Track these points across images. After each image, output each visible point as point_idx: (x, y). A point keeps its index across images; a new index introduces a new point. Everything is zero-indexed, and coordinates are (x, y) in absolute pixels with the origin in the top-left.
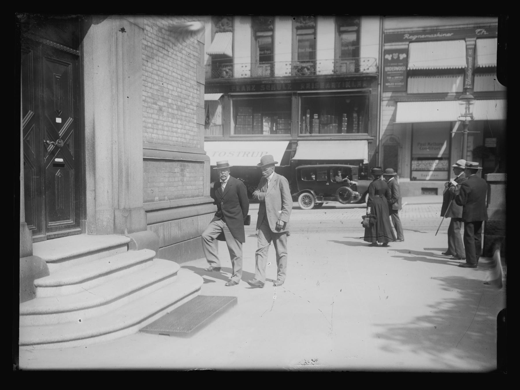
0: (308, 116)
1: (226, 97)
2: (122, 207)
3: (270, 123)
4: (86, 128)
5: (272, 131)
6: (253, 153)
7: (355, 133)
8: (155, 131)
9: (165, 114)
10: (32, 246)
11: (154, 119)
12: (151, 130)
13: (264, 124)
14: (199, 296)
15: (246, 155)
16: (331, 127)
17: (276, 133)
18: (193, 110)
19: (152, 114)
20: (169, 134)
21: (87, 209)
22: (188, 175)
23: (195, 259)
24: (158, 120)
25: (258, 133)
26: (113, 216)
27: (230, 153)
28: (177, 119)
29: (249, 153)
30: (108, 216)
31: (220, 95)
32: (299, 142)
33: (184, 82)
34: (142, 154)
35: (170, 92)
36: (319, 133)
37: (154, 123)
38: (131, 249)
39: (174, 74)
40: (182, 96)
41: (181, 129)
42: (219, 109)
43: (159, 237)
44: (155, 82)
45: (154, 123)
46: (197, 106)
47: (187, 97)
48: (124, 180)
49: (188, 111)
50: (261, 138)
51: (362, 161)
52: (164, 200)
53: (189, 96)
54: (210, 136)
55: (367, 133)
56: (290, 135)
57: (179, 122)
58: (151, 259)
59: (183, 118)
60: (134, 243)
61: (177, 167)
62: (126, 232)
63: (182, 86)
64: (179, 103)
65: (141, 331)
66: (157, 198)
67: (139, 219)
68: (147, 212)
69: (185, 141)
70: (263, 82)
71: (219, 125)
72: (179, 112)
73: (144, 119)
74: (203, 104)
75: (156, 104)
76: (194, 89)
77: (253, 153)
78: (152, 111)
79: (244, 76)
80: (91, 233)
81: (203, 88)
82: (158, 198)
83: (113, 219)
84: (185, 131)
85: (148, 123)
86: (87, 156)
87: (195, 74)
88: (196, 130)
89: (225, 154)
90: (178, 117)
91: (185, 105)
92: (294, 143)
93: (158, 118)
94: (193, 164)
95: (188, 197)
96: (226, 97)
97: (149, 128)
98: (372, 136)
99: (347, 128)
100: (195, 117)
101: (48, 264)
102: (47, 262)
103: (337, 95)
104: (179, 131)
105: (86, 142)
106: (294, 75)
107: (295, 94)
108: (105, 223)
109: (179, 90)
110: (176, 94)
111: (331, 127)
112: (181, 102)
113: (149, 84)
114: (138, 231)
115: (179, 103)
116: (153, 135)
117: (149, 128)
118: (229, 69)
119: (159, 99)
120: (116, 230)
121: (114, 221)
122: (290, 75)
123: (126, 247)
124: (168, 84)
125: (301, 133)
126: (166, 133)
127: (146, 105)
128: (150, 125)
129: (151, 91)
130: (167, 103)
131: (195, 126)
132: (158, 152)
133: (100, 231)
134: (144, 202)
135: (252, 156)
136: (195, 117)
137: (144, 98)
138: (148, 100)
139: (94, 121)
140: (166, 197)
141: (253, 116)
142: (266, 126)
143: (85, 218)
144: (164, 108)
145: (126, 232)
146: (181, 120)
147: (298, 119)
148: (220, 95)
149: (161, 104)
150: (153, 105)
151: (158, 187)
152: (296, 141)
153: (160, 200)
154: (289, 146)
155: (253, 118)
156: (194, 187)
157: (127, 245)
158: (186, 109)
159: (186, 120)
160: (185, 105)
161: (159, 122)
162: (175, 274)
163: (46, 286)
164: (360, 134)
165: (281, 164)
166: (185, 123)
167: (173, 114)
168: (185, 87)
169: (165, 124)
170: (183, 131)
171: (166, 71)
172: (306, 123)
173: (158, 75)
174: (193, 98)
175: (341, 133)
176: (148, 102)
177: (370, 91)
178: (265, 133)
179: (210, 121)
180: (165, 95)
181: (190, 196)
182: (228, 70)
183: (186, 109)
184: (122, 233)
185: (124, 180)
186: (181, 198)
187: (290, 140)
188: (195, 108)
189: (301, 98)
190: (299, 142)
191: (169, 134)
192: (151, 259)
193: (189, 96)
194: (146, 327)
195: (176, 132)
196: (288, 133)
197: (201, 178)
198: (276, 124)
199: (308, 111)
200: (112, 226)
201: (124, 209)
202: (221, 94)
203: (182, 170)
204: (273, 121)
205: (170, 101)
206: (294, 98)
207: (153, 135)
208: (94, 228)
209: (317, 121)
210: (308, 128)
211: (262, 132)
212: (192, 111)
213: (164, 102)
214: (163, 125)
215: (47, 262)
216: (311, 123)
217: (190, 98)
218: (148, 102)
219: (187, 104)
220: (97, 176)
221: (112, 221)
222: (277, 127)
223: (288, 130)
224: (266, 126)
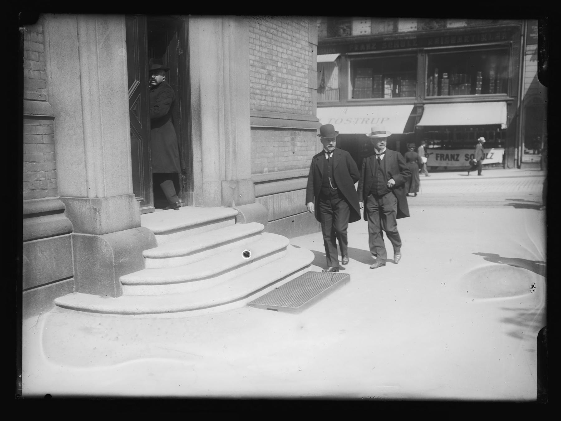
0: (436, 75)
1: (343, 58)
2: (229, 179)
3: (392, 86)
4: (192, 96)
5: (394, 94)
6: (373, 119)
7: (491, 93)
8: (264, 98)
9: (274, 79)
10: (140, 217)
11: (262, 84)
12: (260, 97)
13: (386, 86)
14: (309, 272)
15: (364, 122)
16: (463, 88)
17: (399, 96)
18: (304, 73)
19: (260, 79)
20: (279, 100)
21: (195, 180)
22: (299, 144)
23: (307, 234)
25: (379, 97)
26: (221, 188)
27: (347, 120)
29: (369, 119)
30: (216, 188)
31: (337, 55)
32: (426, 106)
33: (294, 44)
34: (249, 122)
35: (280, 55)
36: (449, 94)
37: (263, 89)
38: (239, 222)
39: (284, 35)
40: (292, 58)
41: (292, 94)
42: (336, 71)
43: (268, 209)
44: (263, 44)
46: (308, 69)
47: (298, 60)
48: (231, 150)
49: (299, 74)
50: (382, 103)
51: (499, 126)
52: (274, 171)
53: (300, 58)
54: (325, 101)
55: (506, 92)
56: (414, 98)
57: (289, 87)
58: (259, 233)
59: (294, 82)
60: (242, 216)
61: (287, 136)
62: (234, 205)
63: (293, 48)
64: (289, 67)
65: (249, 305)
66: (266, 169)
67: (247, 190)
68: (256, 183)
70: (385, 39)
71: (336, 89)
72: (290, 76)
73: (251, 85)
74: (315, 67)
75: (264, 68)
76: (305, 50)
77: (373, 119)
78: (260, 76)
79: (363, 33)
80: (199, 205)
81: (315, 49)
83: (220, 190)
84: (296, 97)
85: (256, 89)
86: (193, 126)
87: (307, 34)
88: (308, 95)
89: (342, 120)
90: (289, 81)
91: (296, 69)
92: (420, 107)
93: (266, 83)
94: (305, 132)
95: (299, 168)
96: (343, 58)
97: (257, 94)
98: (512, 97)
99: (482, 88)
100: (307, 81)
101: (157, 237)
102: (155, 234)
103: (470, 51)
104: (289, 96)
105: (192, 110)
106: (421, 29)
107: (422, 51)
108: (212, 195)
109: (289, 52)
110: (286, 57)
111: (463, 88)
112: (292, 65)
113: (257, 47)
114: (246, 203)
117: (257, 94)
118: (347, 27)
119: (268, 63)
120: (224, 203)
121: (222, 193)
122: (416, 29)
123: (234, 220)
124: (277, 46)
125: (428, 95)
126: (275, 99)
127: (254, 69)
128: (258, 91)
129: (259, 54)
130: (277, 67)
131: (307, 91)
132: (267, 120)
133: (206, 204)
134: (254, 173)
135: (372, 123)
136: (307, 81)
137: (251, 62)
138: (256, 64)
139: (200, 88)
140: (276, 168)
141: (373, 78)
142: (388, 89)
143: (193, 190)
144: (273, 73)
145: (234, 205)
146: (292, 84)
147: (424, 80)
148: (337, 55)
149: (270, 68)
150: (261, 70)
151: (268, 158)
152: (421, 105)
153: (269, 171)
154: (414, 111)
155: (373, 80)
156: (306, 157)
157: (235, 217)
158: (297, 73)
159: (296, 85)
162: (285, 248)
163: (155, 258)
164: (498, 94)
165: (405, 131)
166: (295, 88)
167: (283, 78)
168: (296, 49)
169: (275, 89)
170: (293, 96)
171: (275, 32)
172: (434, 84)
173: (267, 37)
174: (305, 60)
175: (474, 94)
176: (256, 67)
177: (511, 44)
178: (386, 97)
179: (325, 85)
180: (274, 58)
181: (302, 166)
182: (345, 28)
183: (297, 73)
184: (230, 205)
185: (231, 150)
186: (292, 169)
187: (414, 104)
188: (307, 71)
189: (428, 56)
190: (426, 106)
191: (279, 100)
192: (259, 233)
193: (300, 58)
194: (254, 301)
195: (287, 98)
196: (413, 96)
197: (314, 148)
198: (399, 86)
199: (437, 70)
200: (220, 198)
201: (232, 180)
202: (338, 55)
203: (293, 139)
204: (395, 83)
205: (279, 64)
206: (420, 56)
207: (262, 102)
208: (202, 200)
209: (447, 81)
210: (436, 89)
211: (383, 95)
212: (303, 75)
213: (273, 66)
214: (272, 91)
215: (155, 234)
216: (440, 83)
217: (302, 60)
218: (256, 67)
219: (298, 67)
220: (204, 147)
221: (219, 193)
222: (400, 90)
223: (412, 93)
224: (388, 89)
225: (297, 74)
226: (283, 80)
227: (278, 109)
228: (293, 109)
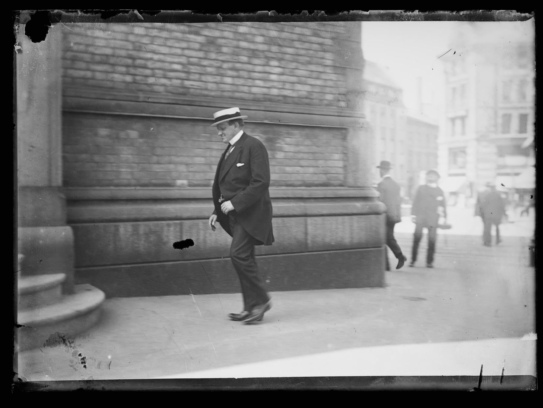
12: (183, 75)
24: (205, 58)
28: (267, 58)
41: (282, 74)
57: (274, 63)
69: (294, 94)
72: (274, 49)
78: (184, 45)
84: (294, 79)
90: (270, 55)
100: (328, 55)
116: (187, 83)
126: (228, 80)
146: (280, 60)
150: (188, 36)
151: (187, 164)
160: (295, 37)
167: (253, 50)
170: (284, 78)
188: (328, 42)
191: (241, 81)
207: (187, 83)
225: (297, 44)
226: (254, 53)
227: (237, 95)
228: (285, 97)
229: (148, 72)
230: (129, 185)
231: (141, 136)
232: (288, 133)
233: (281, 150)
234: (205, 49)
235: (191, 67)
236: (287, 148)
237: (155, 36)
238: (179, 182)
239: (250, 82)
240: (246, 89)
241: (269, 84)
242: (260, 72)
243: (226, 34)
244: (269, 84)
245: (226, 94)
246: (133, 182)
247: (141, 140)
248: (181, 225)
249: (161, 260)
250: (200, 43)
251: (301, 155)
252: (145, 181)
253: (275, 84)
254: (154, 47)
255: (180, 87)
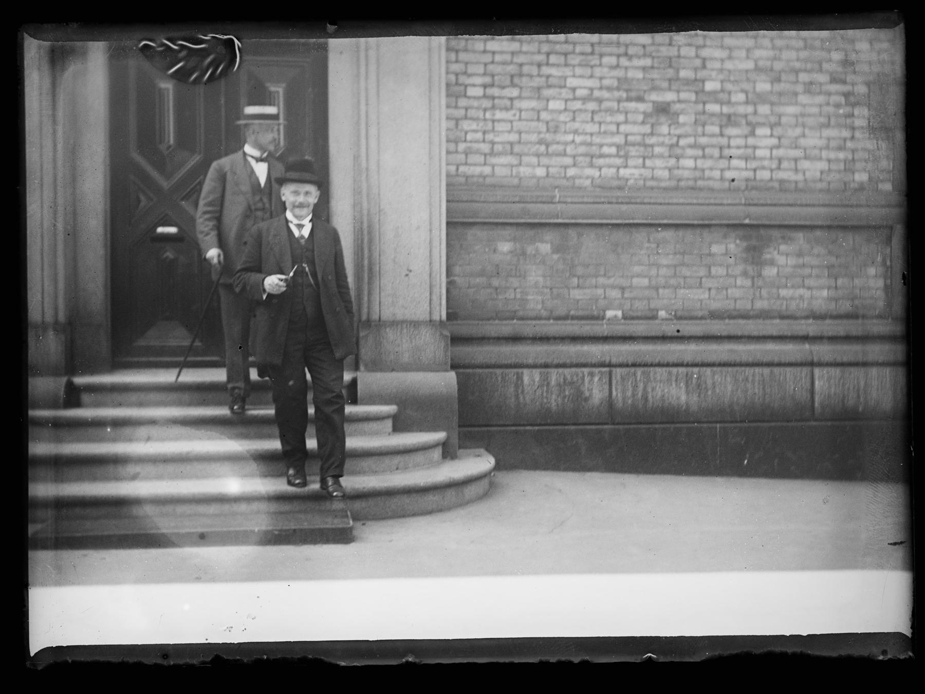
12: (618, 161)
24: (652, 134)
45: (633, 145)
69: (800, 177)
72: (764, 109)
75: (640, 99)
78: (621, 118)
82: (619, 314)
84: (798, 153)
110: (750, 65)
115: (763, 86)
117: (602, 156)
119: (654, 88)
126: (690, 163)
127: (592, 106)
130: (700, 92)
137: (580, 93)
161: (653, 140)
191: (708, 163)
205: (709, 86)
218: (600, 101)
225: (803, 99)
227: (700, 183)
228: (781, 182)
229: (568, 161)
230: (540, 318)
231: (556, 250)
232: (783, 238)
233: (772, 263)
234: (653, 120)
235: (631, 148)
236: (781, 260)
237: (580, 110)
238: (610, 314)
239: (723, 163)
240: (717, 174)
241: (754, 164)
242: (738, 147)
243: (683, 96)
244: (754, 164)
245: (682, 184)
246: (544, 313)
247: (555, 257)
248: (610, 373)
249: (580, 422)
250: (644, 113)
251: (807, 271)
252: (561, 311)
253: (766, 163)
254: (577, 125)
255: (612, 178)
